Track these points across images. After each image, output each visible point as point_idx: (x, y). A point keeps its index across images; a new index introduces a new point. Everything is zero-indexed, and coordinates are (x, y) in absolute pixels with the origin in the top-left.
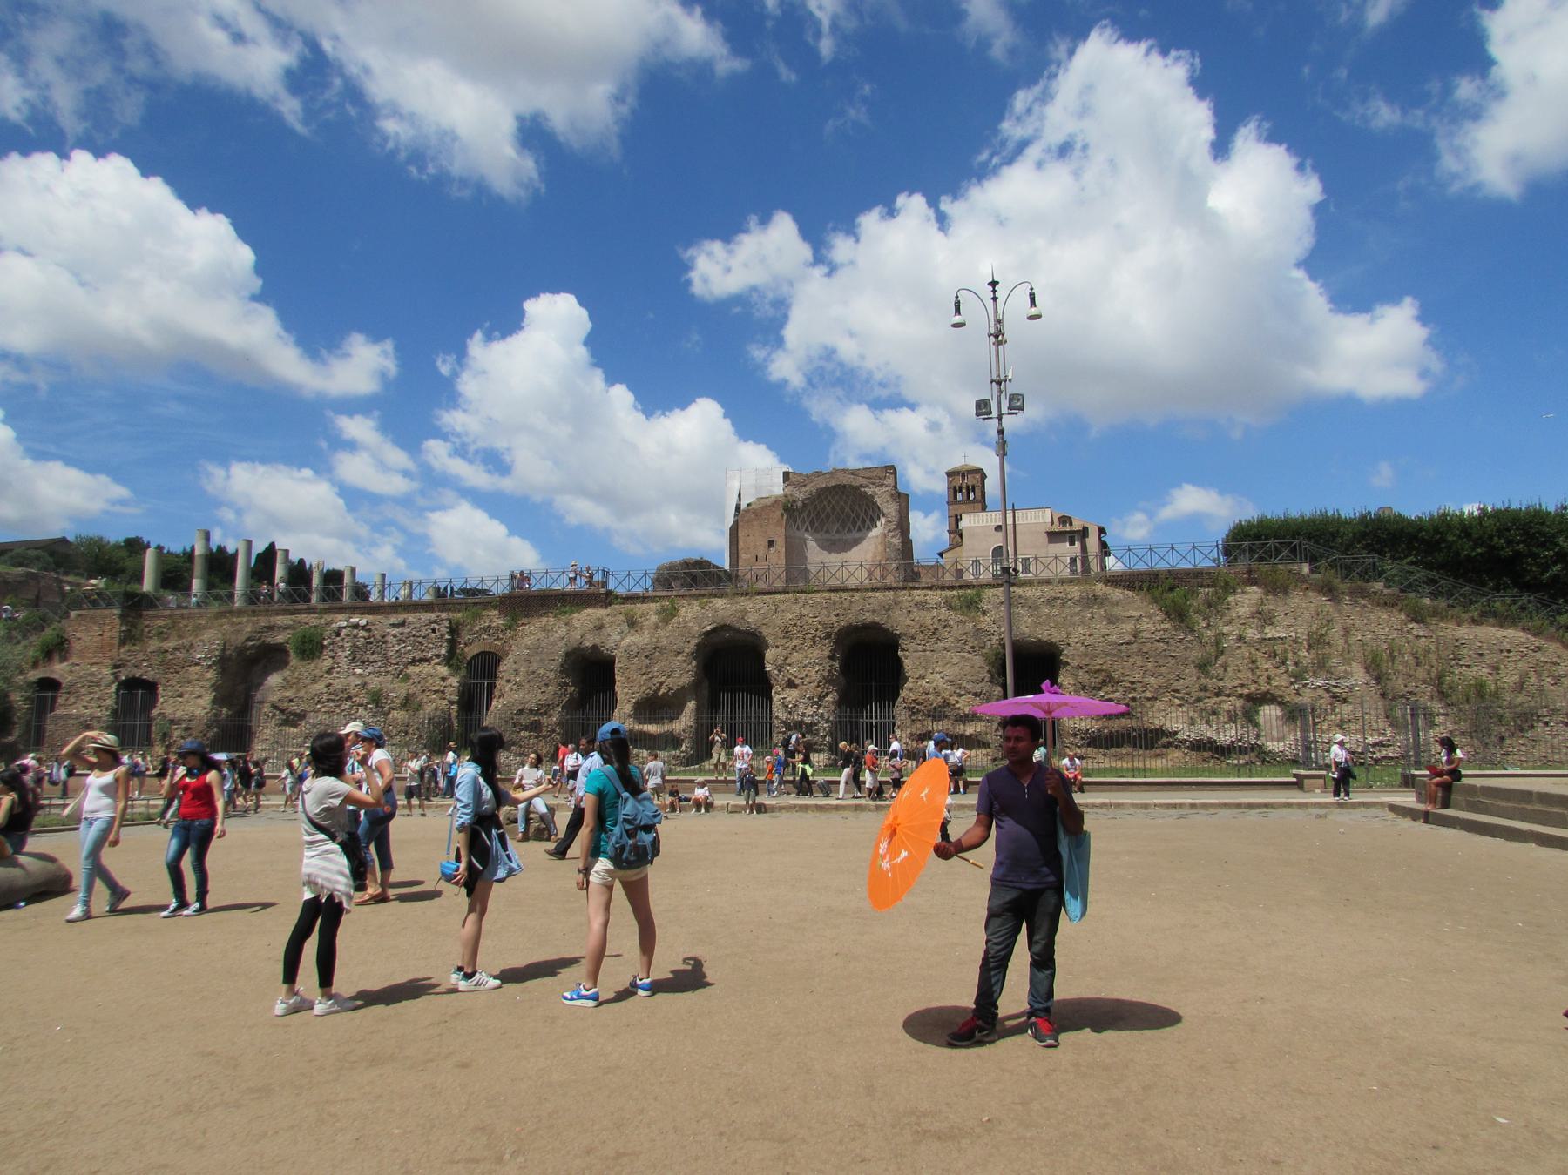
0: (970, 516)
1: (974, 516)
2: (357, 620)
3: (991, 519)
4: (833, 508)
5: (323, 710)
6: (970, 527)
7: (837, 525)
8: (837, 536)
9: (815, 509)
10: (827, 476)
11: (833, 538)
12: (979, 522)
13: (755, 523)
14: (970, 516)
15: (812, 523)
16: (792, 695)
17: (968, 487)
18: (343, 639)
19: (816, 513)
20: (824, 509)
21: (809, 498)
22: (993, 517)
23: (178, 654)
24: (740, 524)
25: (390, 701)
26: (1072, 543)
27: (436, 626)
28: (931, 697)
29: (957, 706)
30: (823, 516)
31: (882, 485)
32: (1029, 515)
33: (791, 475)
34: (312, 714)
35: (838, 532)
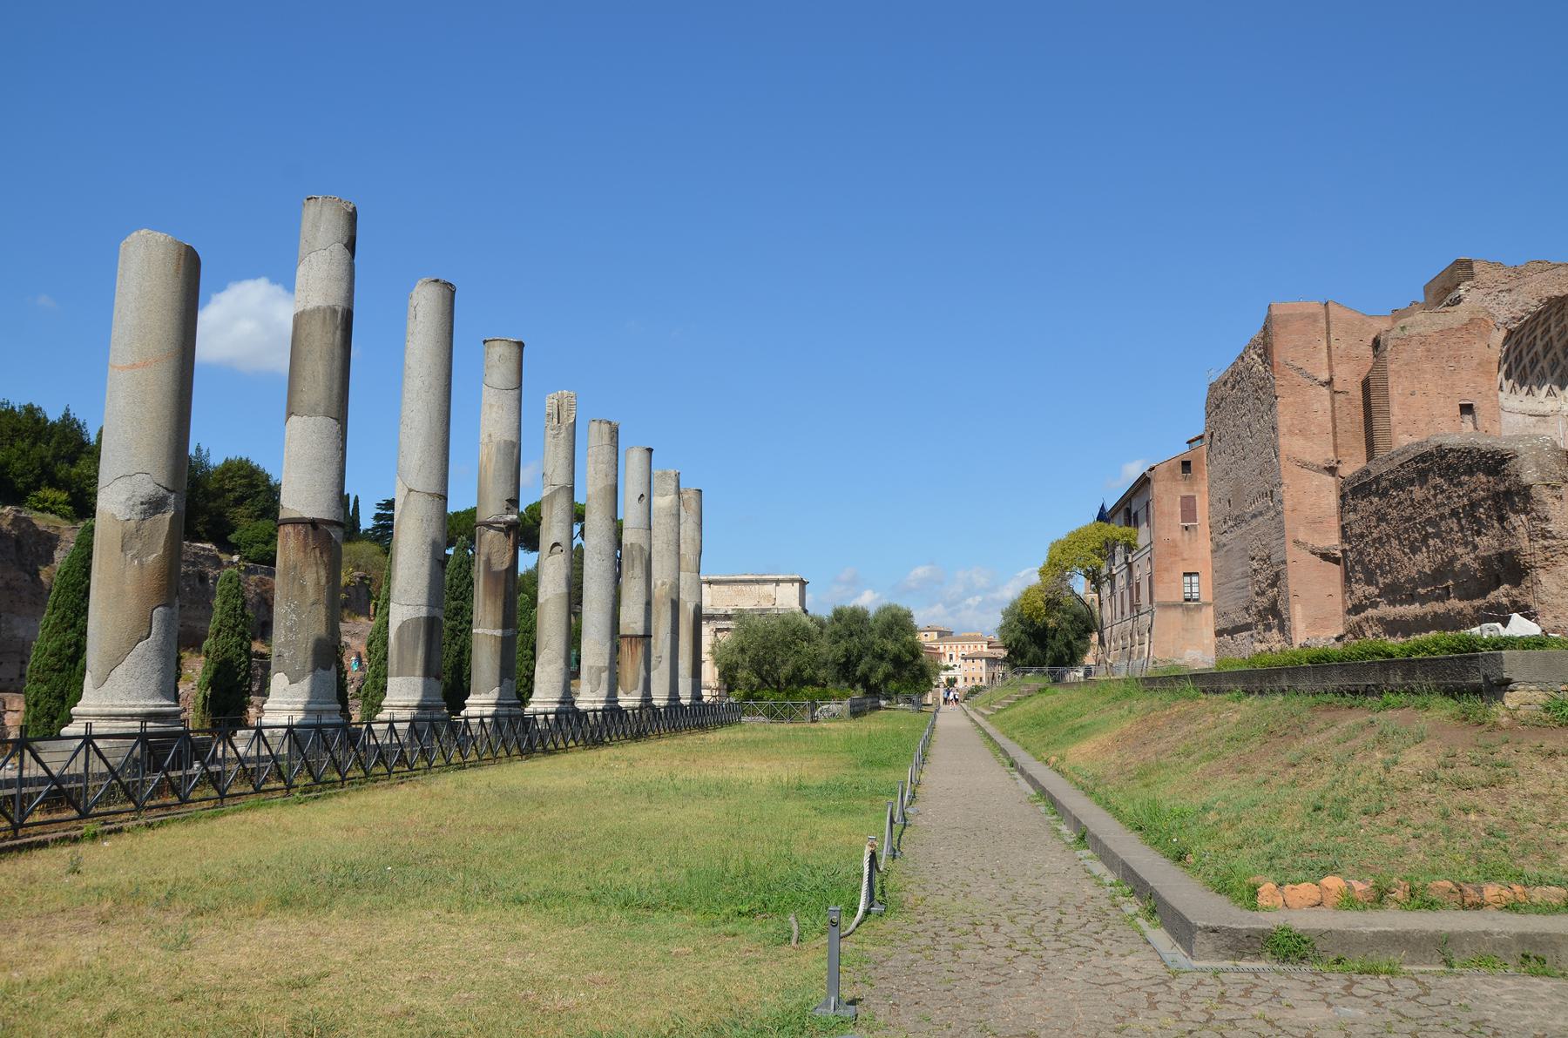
9: (1518, 343)
11: (1541, 409)
13: (1427, 366)
15: (1508, 376)
19: (1517, 351)
20: (1532, 345)
21: (1523, 317)
30: (1526, 360)
33: (1476, 268)
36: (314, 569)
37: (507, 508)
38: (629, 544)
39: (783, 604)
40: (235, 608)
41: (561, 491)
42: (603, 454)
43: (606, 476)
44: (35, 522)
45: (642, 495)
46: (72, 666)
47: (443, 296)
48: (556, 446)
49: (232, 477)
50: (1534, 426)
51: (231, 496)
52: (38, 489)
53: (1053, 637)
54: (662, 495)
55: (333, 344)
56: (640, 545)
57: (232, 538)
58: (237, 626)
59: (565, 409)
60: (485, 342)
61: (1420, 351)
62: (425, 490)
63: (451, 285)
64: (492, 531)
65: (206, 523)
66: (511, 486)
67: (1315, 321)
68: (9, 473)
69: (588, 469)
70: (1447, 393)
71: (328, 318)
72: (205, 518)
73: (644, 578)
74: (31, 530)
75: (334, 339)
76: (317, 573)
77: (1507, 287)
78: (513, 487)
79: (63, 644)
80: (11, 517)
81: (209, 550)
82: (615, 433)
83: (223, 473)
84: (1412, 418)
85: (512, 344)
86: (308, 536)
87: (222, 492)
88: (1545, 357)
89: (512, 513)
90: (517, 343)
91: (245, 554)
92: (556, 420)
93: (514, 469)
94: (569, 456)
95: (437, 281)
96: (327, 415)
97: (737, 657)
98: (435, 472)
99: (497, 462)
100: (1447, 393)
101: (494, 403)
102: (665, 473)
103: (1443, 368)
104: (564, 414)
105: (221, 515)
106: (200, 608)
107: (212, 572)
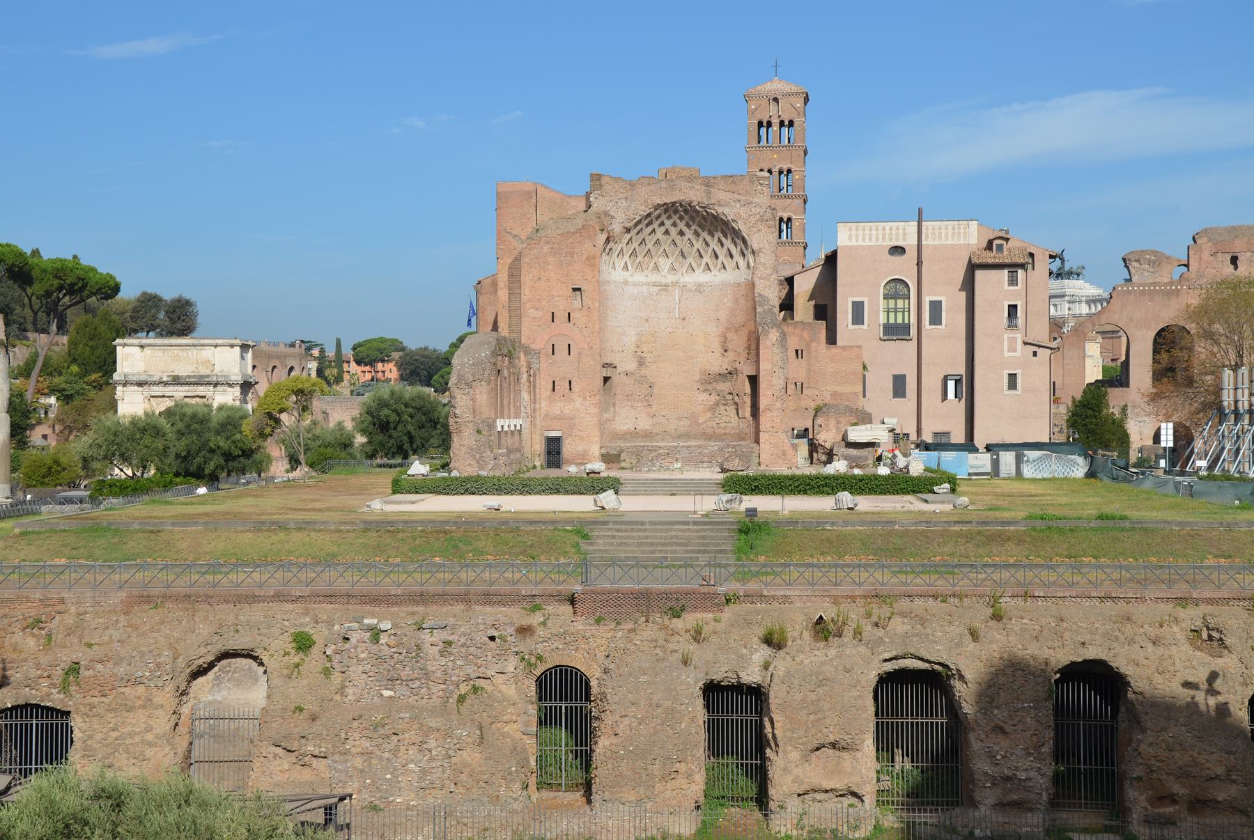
0: (850, 229)
1: (857, 229)
2: (375, 621)
3: (884, 235)
4: (667, 232)
5: (354, 750)
6: (851, 247)
7: (671, 260)
8: (670, 278)
10: (664, 184)
11: (663, 281)
12: (864, 240)
13: (551, 259)
14: (850, 229)
16: (1000, 745)
17: (782, 124)
18: (355, 648)
21: (635, 219)
22: (888, 231)
23: (99, 667)
24: (526, 260)
25: (456, 741)
26: (1013, 281)
27: (496, 634)
28: (1177, 755)
29: (1207, 765)
31: (751, 203)
32: (943, 232)
33: (604, 180)
34: (336, 757)
35: (673, 269)
39: (222, 371)
50: (657, 294)
53: (395, 428)
61: (546, 248)
67: (530, 197)
70: (564, 279)
77: (624, 196)
84: (538, 297)
88: (666, 243)
97: (93, 452)
100: (564, 279)
103: (561, 261)
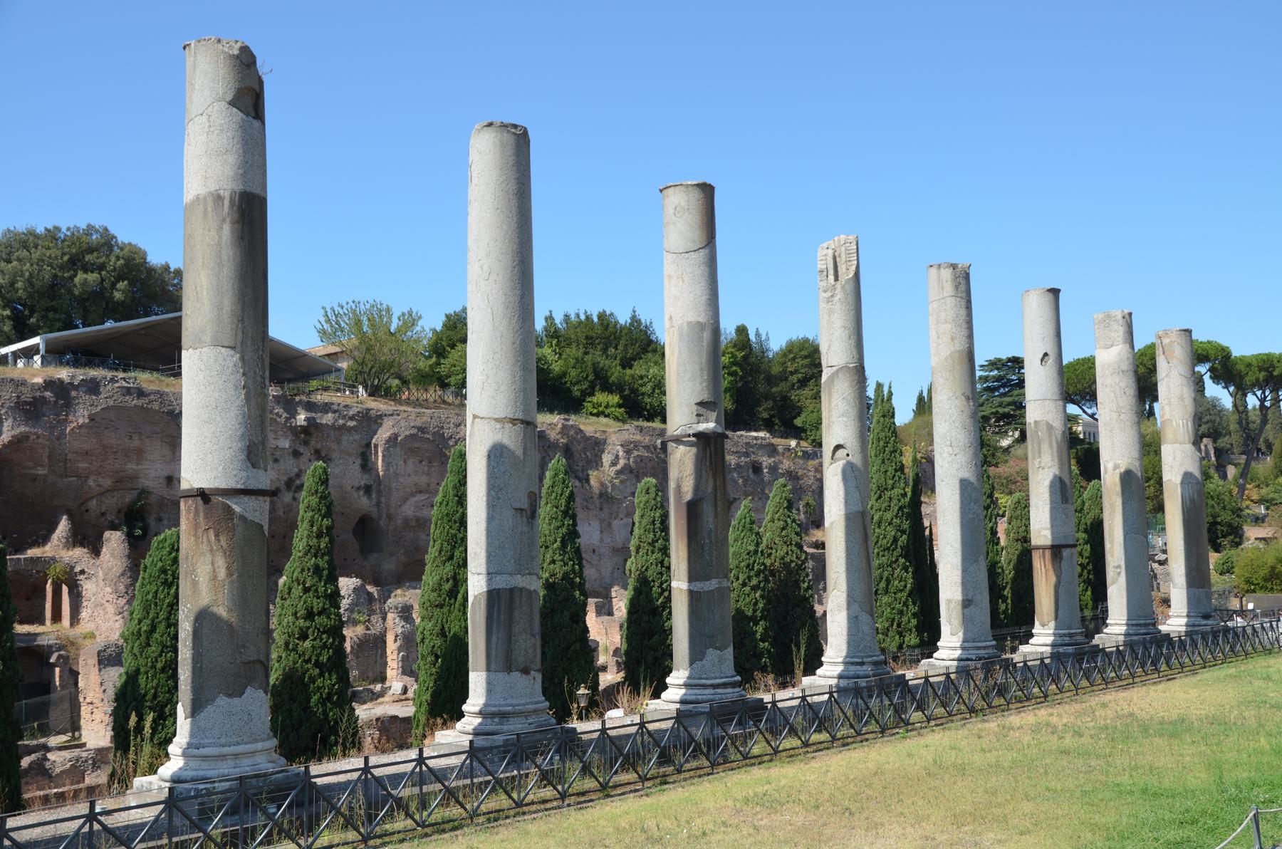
36: (209, 558)
37: (698, 415)
38: (1032, 422)
40: (654, 521)
41: (841, 375)
42: (945, 310)
43: (952, 339)
44: (582, 427)
45: (1046, 354)
46: (453, 600)
47: (502, 145)
48: (830, 313)
49: (794, 359)
51: (794, 378)
52: (592, 394)
54: (1107, 347)
55: (219, 244)
56: (1047, 423)
57: (798, 422)
58: (657, 541)
59: (844, 260)
60: (661, 191)
62: (490, 416)
63: (515, 126)
64: (681, 447)
65: (772, 409)
66: (701, 383)
68: (566, 382)
69: (930, 333)
71: (209, 209)
72: (769, 404)
73: (1057, 466)
74: (579, 436)
75: (220, 237)
76: (213, 565)
78: (705, 384)
79: (442, 578)
80: (560, 426)
81: (762, 438)
82: (963, 280)
83: (785, 355)
85: (690, 188)
86: (199, 517)
87: (783, 377)
89: (707, 421)
90: (698, 185)
91: (812, 438)
92: (831, 277)
93: (704, 361)
94: (851, 325)
95: (490, 125)
96: (216, 344)
98: (503, 388)
99: (680, 353)
101: (672, 274)
102: (1108, 316)
104: (842, 269)
105: (785, 398)
106: (756, 499)
107: (766, 461)
